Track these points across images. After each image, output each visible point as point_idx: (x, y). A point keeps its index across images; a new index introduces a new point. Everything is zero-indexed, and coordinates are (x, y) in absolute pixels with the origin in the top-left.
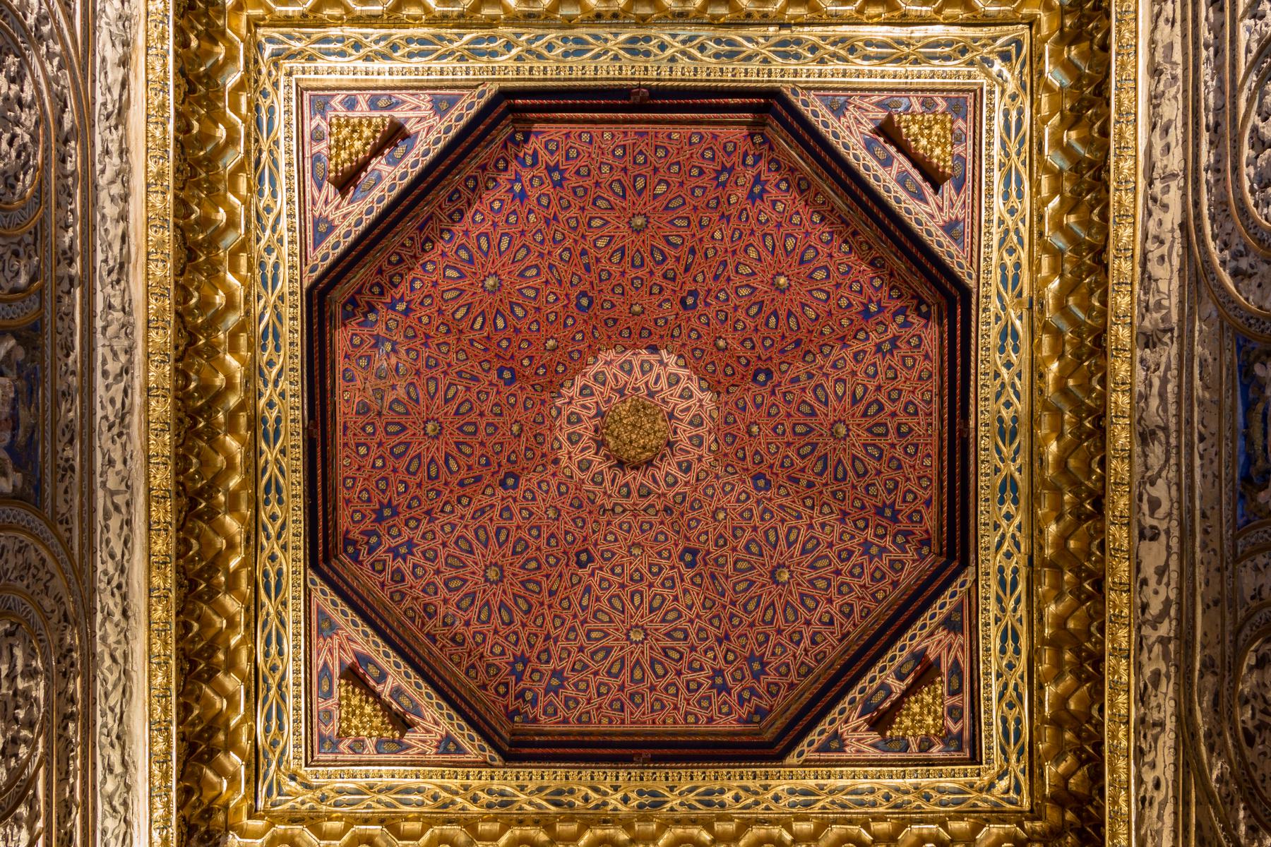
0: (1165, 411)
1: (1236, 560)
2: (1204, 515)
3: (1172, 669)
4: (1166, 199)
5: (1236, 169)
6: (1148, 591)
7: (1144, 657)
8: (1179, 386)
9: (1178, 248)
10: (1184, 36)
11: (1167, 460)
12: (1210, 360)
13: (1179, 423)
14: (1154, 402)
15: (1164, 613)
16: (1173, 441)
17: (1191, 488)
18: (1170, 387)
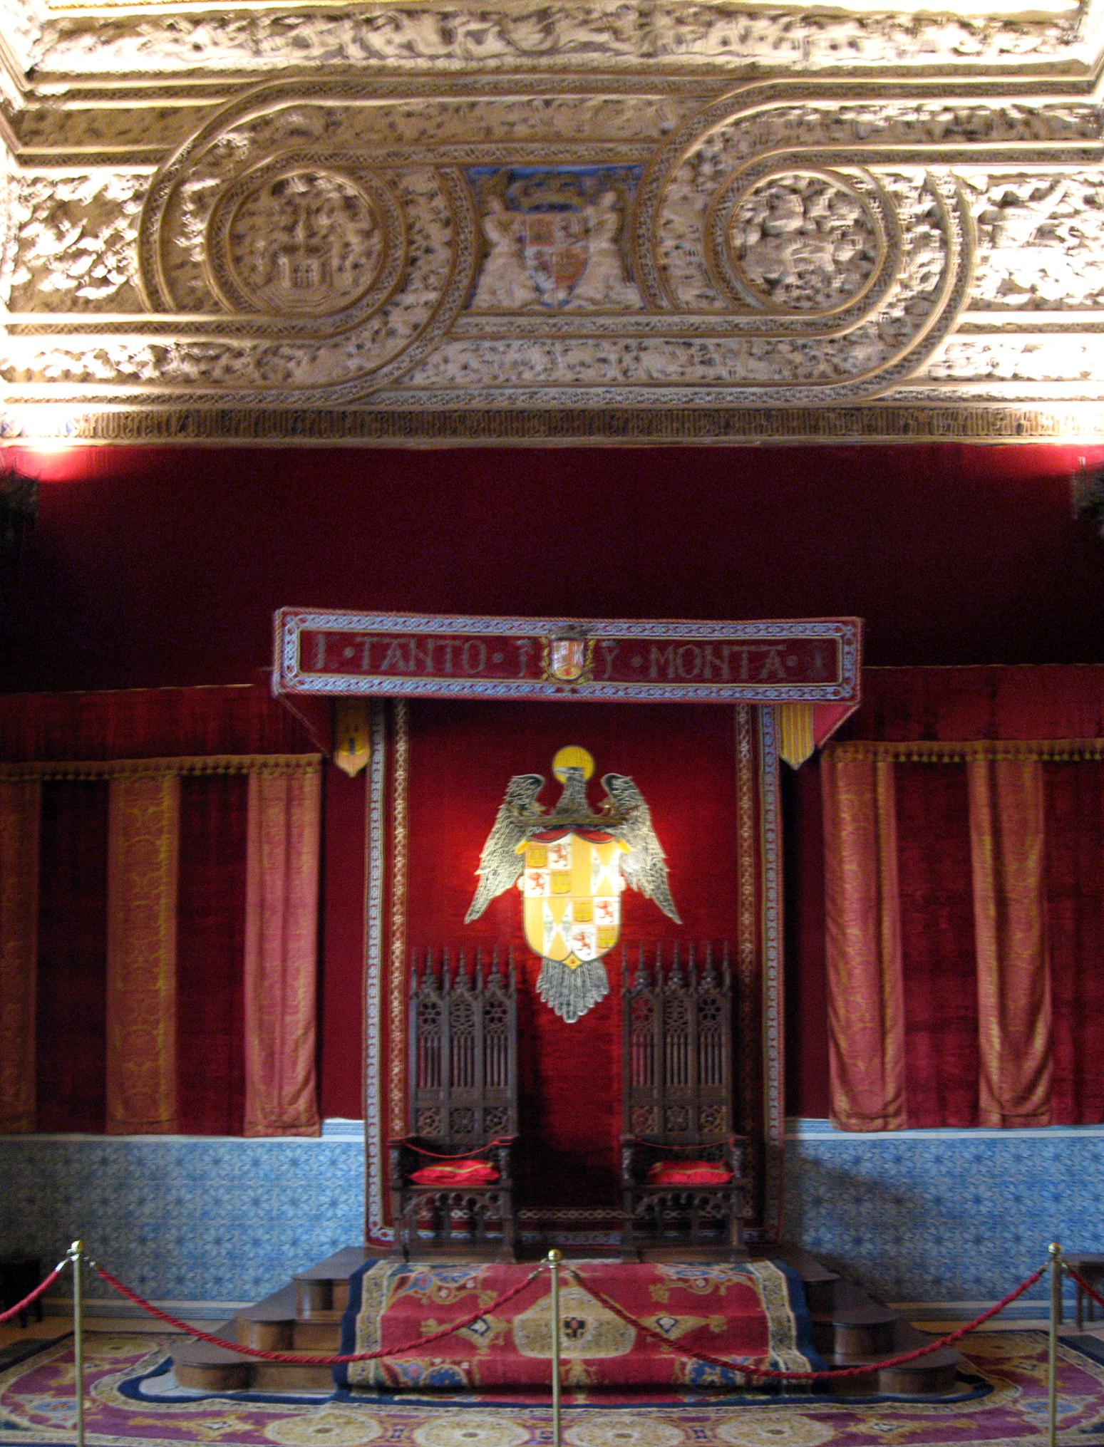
0: (574, 50)
1: (438, 166)
2: (473, 106)
3: (318, 63)
4: (786, 46)
5: (797, 161)
6: (388, 31)
7: (323, 26)
8: (595, 70)
9: (735, 62)
10: (939, 71)
11: (525, 53)
12: (619, 121)
13: (565, 69)
14: (583, 36)
15: (371, 52)
16: (544, 61)
17: (496, 90)
18: (596, 55)
